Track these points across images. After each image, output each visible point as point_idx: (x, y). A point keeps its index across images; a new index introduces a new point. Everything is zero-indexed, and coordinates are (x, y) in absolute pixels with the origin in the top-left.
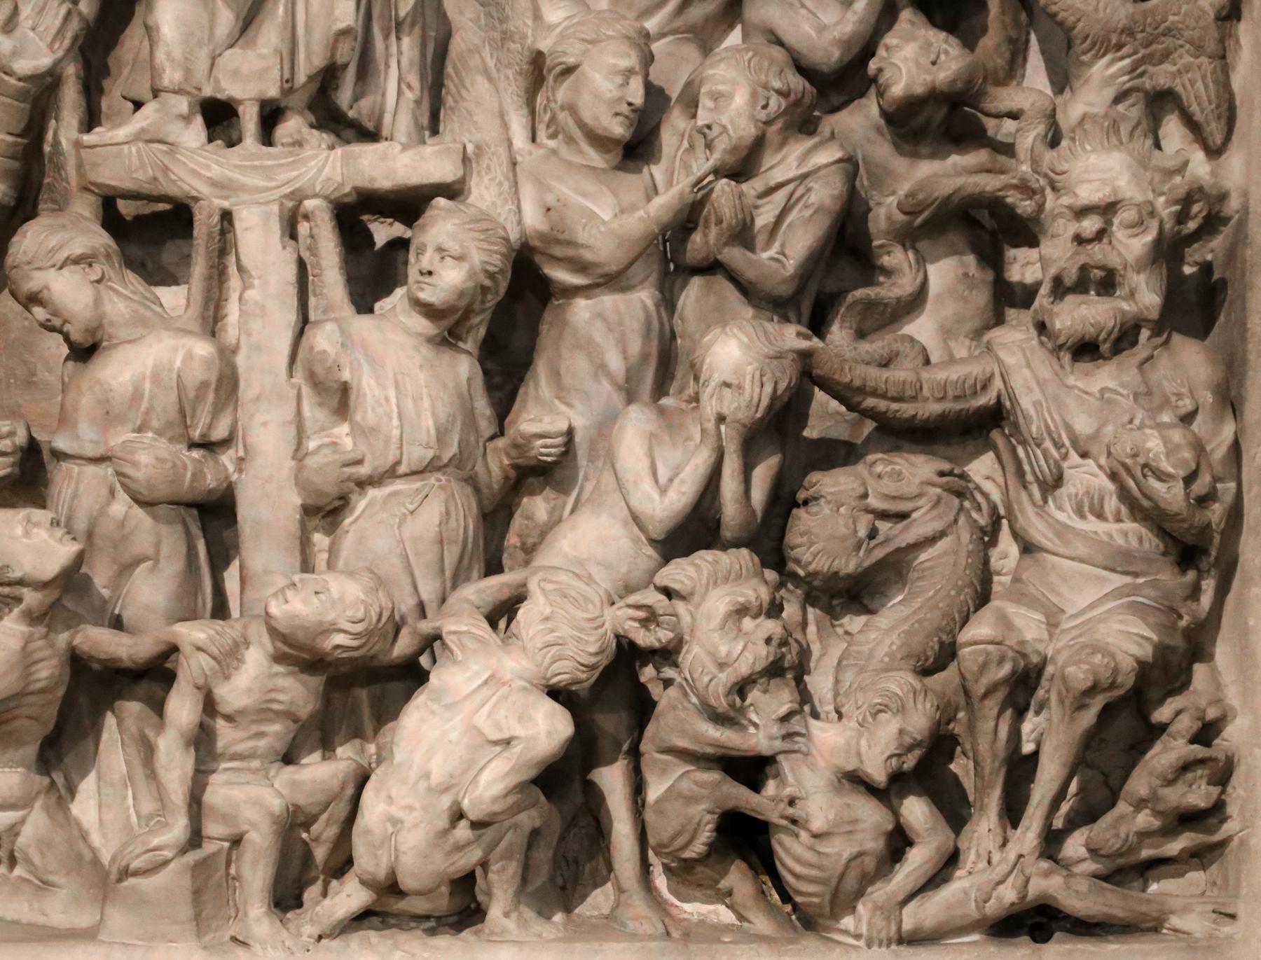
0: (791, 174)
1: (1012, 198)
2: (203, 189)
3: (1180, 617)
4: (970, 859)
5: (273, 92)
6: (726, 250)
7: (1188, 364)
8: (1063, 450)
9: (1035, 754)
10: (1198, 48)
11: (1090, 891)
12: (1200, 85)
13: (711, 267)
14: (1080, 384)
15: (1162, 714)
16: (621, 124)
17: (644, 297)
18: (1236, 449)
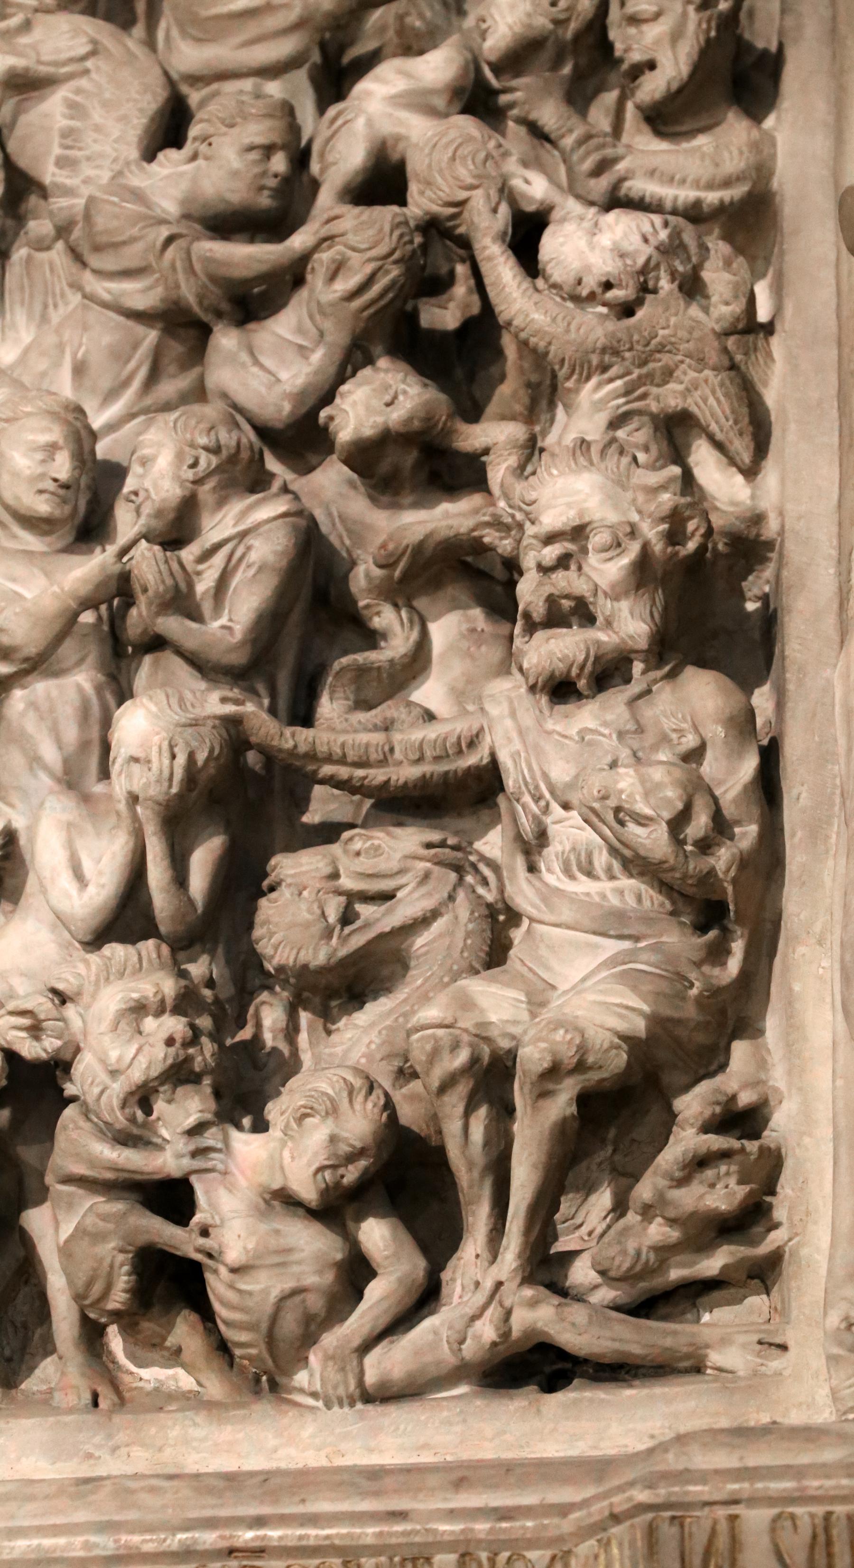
0: (226, 534)
1: (489, 537)
3: (692, 985)
6: (160, 620)
7: (699, 698)
8: (542, 803)
11: (590, 1322)
12: (711, 401)
14: (558, 728)
16: (47, 501)
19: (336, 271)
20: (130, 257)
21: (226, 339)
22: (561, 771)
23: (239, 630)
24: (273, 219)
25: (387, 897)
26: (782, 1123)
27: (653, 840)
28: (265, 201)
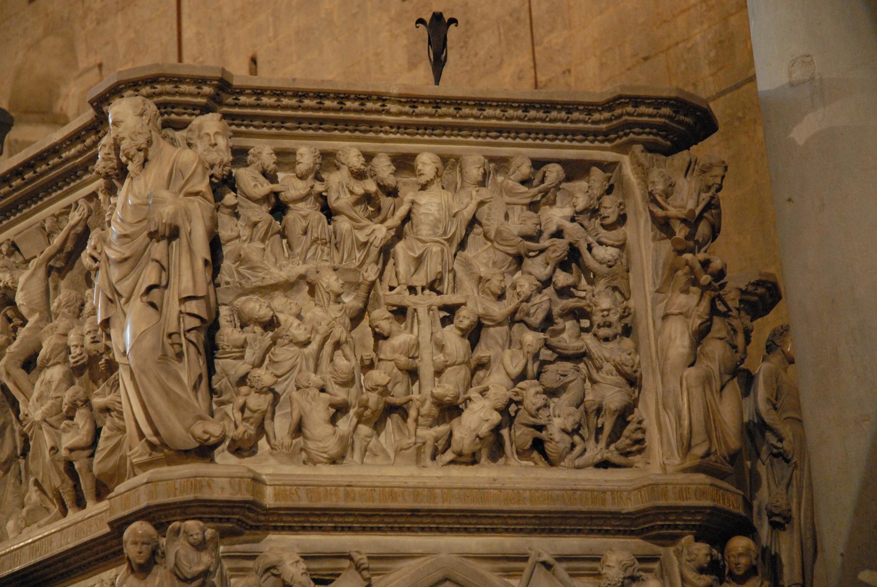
1: (586, 308)
2: (410, 304)
4: (588, 450)
7: (628, 343)
10: (622, 278)
13: (522, 321)
15: (629, 418)
17: (506, 327)
18: (639, 363)
19: (555, 251)
20: (509, 243)
21: (527, 262)
22: (607, 355)
23: (538, 321)
24: (534, 238)
26: (645, 424)
28: (535, 234)
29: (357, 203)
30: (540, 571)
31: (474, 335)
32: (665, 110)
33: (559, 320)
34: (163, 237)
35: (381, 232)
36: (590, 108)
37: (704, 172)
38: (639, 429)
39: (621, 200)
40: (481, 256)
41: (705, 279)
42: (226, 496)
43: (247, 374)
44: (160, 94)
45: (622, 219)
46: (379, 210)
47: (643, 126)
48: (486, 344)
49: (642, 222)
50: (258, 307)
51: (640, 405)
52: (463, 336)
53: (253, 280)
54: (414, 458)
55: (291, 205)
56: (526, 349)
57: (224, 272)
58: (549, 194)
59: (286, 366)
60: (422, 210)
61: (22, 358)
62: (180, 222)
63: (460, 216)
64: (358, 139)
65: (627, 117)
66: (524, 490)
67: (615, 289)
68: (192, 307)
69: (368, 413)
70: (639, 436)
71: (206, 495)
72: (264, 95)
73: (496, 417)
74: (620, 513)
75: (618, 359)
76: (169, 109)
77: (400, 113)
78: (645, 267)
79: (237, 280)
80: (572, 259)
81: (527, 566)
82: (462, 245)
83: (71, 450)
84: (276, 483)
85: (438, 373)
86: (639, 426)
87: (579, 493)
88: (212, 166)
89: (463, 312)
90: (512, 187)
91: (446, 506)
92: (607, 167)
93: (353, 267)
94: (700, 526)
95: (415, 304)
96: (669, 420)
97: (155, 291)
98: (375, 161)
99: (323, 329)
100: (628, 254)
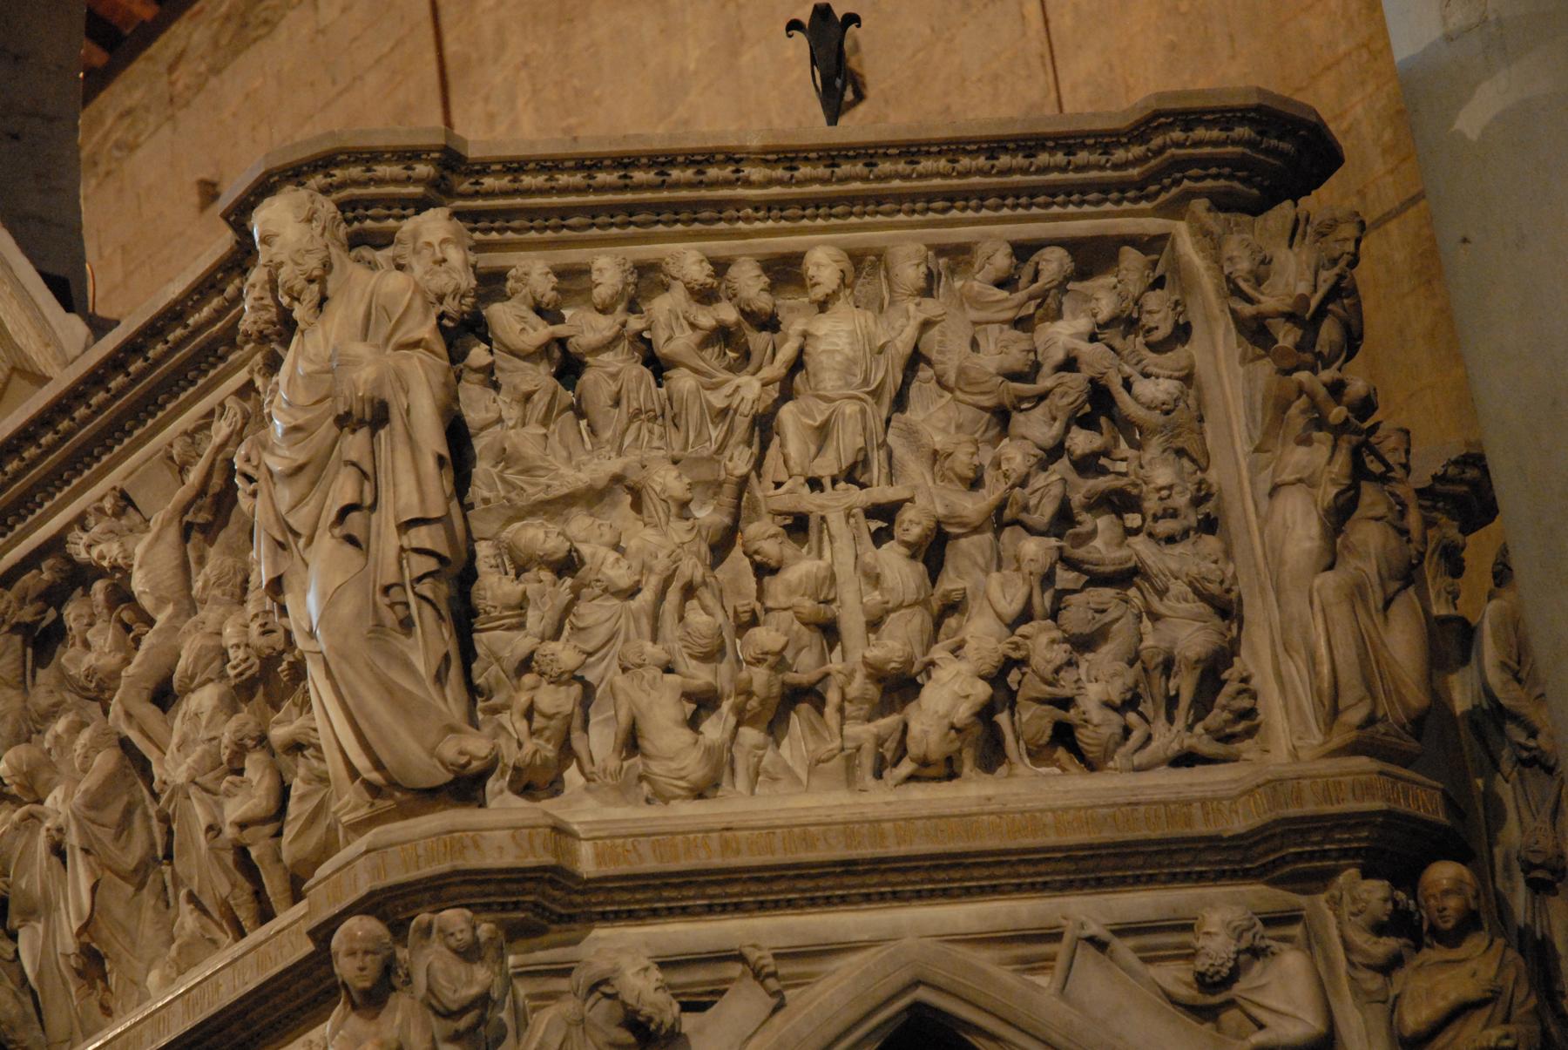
1: (1129, 489)
5: (836, 472)
7: (1211, 543)
9: (1177, 695)
10: (1192, 431)
13: (1016, 522)
15: (1225, 675)
17: (989, 536)
18: (1235, 577)
19: (1063, 396)
21: (1017, 418)
22: (1174, 566)
23: (1046, 519)
25: (1103, 611)
26: (1255, 683)
27: (1214, 588)
28: (1027, 369)
29: (705, 344)
30: (1087, 955)
31: (933, 551)
32: (1242, 131)
33: (1084, 517)
34: (361, 423)
35: (750, 389)
36: (1106, 141)
37: (1324, 235)
38: (1245, 691)
39: (1176, 297)
40: (935, 417)
41: (1337, 413)
42: (508, 861)
43: (532, 653)
44: (342, 185)
45: (1182, 333)
46: (746, 356)
47: (1204, 162)
48: (956, 569)
49: (1220, 333)
50: (541, 535)
51: (1243, 652)
52: (913, 557)
53: (530, 490)
54: (843, 777)
55: (588, 359)
56: (1026, 569)
57: (478, 482)
58: (1049, 300)
59: (601, 634)
60: (822, 347)
61: (151, 685)
62: (388, 394)
63: (890, 351)
64: (698, 236)
65: (1173, 150)
66: (1042, 811)
67: (1180, 452)
68: (422, 537)
69: (753, 703)
70: (1245, 703)
71: (472, 861)
72: (526, 172)
73: (982, 690)
74: (1217, 839)
75: (1194, 571)
76: (361, 211)
77: (769, 183)
78: (1232, 410)
79: (502, 493)
80: (1099, 404)
81: (1061, 949)
82: (900, 402)
83: (242, 825)
84: (596, 834)
85: (874, 625)
86: (1243, 686)
87: (1142, 809)
88: (441, 299)
89: (908, 514)
90: (979, 293)
91: (903, 850)
92: (1151, 245)
93: (706, 453)
94: (1367, 849)
95: (822, 507)
96: (1296, 671)
97: (355, 516)
98: (733, 272)
99: (661, 564)
100: (1199, 389)
